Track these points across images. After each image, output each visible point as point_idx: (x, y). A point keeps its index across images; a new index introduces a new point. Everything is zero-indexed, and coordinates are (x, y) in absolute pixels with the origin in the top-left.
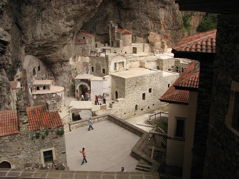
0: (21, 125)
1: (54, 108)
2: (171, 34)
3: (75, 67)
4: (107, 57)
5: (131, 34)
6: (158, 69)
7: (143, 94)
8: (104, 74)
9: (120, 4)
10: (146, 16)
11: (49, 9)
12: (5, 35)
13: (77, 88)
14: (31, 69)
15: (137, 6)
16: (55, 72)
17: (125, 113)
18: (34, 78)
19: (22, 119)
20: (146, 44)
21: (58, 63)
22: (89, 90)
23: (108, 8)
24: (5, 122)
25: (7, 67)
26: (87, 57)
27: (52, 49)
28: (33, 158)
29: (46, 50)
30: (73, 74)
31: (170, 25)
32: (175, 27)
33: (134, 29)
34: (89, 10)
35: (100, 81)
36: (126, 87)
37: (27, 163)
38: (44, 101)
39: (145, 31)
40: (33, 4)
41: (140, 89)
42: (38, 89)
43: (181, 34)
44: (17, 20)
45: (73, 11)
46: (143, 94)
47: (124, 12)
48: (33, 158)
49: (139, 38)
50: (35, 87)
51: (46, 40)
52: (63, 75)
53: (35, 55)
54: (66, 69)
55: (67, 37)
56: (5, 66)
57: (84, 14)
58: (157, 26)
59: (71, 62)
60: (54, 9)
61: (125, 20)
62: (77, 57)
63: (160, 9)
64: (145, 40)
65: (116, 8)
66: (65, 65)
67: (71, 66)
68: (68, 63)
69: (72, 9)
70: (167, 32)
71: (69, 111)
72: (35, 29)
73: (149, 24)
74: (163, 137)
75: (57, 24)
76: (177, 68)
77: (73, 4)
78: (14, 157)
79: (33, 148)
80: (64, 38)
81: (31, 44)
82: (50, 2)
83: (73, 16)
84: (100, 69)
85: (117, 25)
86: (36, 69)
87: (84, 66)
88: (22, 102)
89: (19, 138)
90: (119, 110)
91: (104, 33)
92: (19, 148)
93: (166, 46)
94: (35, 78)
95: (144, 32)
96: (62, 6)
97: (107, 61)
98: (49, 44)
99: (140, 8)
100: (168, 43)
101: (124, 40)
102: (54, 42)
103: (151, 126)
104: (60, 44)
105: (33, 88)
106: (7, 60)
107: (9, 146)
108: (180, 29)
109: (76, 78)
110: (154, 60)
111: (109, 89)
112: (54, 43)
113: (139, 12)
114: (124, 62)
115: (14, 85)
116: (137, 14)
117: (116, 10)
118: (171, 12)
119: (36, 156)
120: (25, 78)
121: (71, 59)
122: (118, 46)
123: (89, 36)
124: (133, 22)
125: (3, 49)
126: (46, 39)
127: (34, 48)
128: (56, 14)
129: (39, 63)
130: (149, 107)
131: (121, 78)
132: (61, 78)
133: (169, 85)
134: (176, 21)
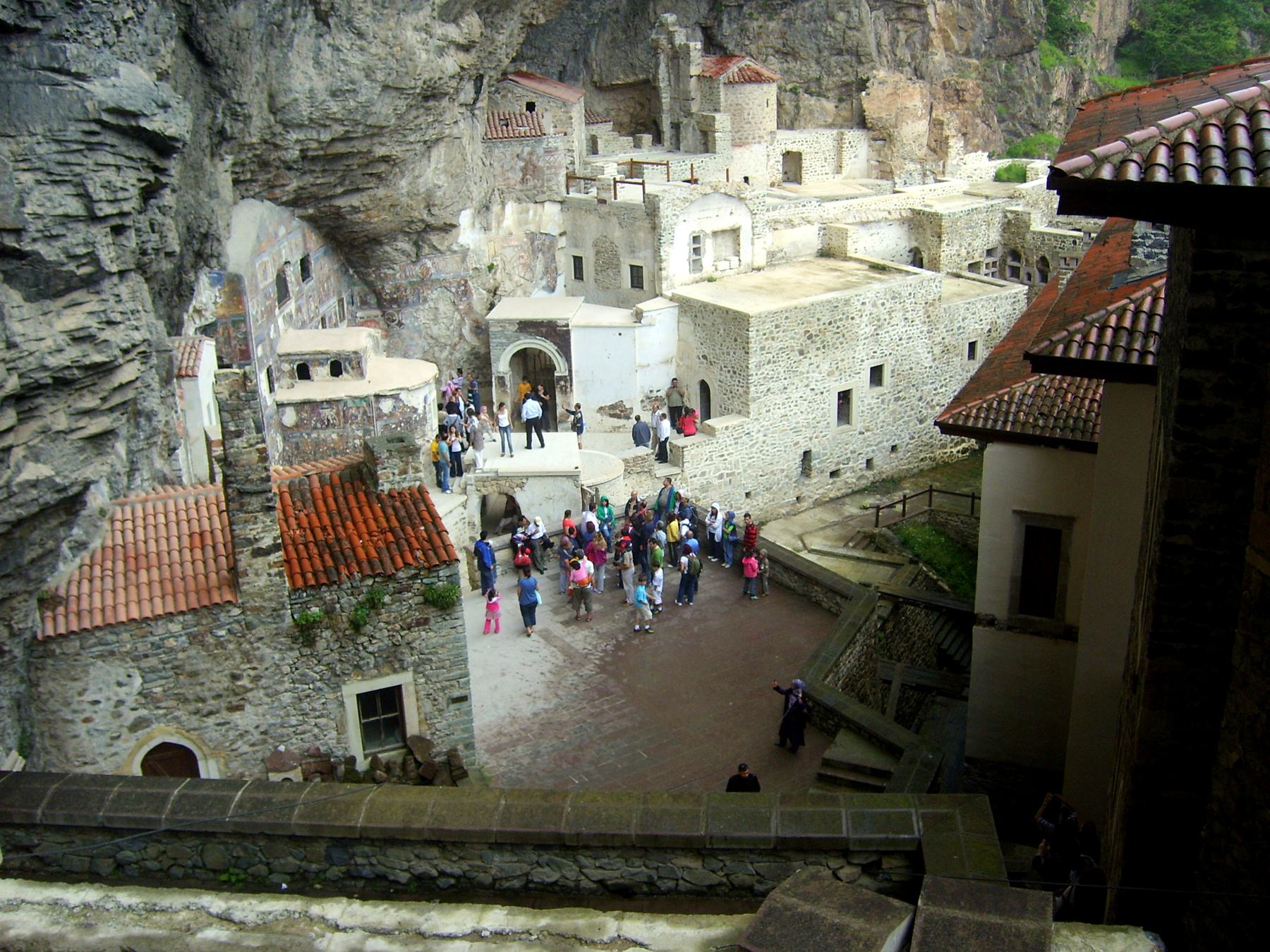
0: (244, 559)
1: (404, 472)
2: (984, 79)
3: (486, 261)
4: (651, 208)
5: (769, 80)
6: (914, 263)
8: (636, 292)
12: (165, 106)
13: (502, 365)
14: (265, 271)
16: (388, 288)
17: (748, 495)
18: (280, 320)
19: (251, 531)
20: (855, 137)
21: (400, 237)
22: (561, 378)
24: (164, 547)
25: (154, 267)
26: (547, 204)
27: (367, 165)
28: (306, 727)
29: (340, 174)
30: (479, 297)
31: (978, 30)
32: (1005, 39)
33: (786, 53)
35: (620, 331)
36: (753, 361)
37: (276, 753)
38: (334, 436)
41: (825, 367)
42: (303, 372)
43: (1033, 79)
44: (191, 19)
48: (306, 727)
49: (813, 101)
50: (286, 367)
51: (340, 121)
52: (425, 300)
53: (285, 199)
54: (442, 267)
55: (445, 102)
56: (146, 259)
58: (908, 38)
59: (468, 234)
62: (496, 208)
66: (435, 248)
67: (465, 253)
68: (449, 238)
71: (466, 485)
72: (284, 66)
73: (869, 28)
76: (1016, 255)
78: (211, 721)
81: (266, 142)
84: (618, 266)
85: (699, 34)
86: (293, 274)
88: (251, 446)
89: (236, 626)
90: (721, 477)
91: (631, 79)
92: (235, 677)
93: (956, 144)
95: (842, 69)
97: (654, 227)
98: (355, 143)
101: (737, 113)
103: (885, 558)
104: (412, 138)
105: (279, 370)
106: (156, 228)
108: (1030, 49)
109: (493, 315)
110: (896, 215)
111: (664, 368)
112: (383, 135)
115: (186, 356)
119: (321, 716)
120: (239, 320)
121: (465, 218)
122: (705, 144)
124: (784, 16)
125: (151, 177)
126: (339, 116)
130: (869, 462)
131: (727, 311)
132: (417, 318)
133: (972, 346)
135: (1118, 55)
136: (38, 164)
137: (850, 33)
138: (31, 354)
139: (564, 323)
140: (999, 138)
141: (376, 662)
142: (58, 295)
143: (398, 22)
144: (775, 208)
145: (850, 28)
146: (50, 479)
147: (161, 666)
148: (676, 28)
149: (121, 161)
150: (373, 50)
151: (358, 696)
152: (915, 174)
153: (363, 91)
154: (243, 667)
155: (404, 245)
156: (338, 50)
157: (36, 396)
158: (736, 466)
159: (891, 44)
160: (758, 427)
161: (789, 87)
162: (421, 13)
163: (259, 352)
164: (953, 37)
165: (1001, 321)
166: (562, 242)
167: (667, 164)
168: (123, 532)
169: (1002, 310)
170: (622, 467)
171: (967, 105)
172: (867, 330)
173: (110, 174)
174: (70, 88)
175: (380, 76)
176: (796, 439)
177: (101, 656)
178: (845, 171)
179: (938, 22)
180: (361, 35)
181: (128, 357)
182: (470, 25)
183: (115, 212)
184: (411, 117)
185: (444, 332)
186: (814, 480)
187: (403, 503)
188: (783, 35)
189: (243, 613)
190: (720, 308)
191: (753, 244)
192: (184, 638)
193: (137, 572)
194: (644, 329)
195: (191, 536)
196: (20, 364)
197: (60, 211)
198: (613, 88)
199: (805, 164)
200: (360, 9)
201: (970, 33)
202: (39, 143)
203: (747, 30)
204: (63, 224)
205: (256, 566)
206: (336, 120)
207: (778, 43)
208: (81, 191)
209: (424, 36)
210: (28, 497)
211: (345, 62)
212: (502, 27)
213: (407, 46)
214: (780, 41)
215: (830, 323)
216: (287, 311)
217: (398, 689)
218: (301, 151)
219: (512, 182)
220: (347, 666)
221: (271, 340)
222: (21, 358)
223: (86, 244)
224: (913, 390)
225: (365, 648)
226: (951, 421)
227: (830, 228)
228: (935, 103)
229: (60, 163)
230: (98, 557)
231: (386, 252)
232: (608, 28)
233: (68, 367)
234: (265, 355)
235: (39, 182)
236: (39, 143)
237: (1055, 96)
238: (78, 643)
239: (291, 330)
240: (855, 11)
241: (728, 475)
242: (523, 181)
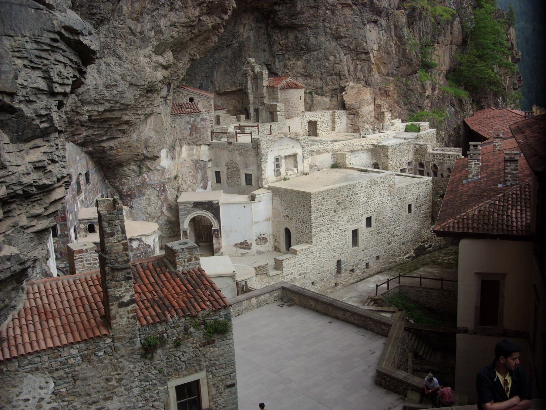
0: (114, 309)
1: (190, 260)
3: (174, 175)
4: (256, 145)
5: (301, 87)
7: (353, 231)
8: (249, 187)
9: (272, 16)
10: (334, 43)
11: (116, 21)
13: (185, 225)
15: (314, 19)
16: (125, 189)
17: (313, 283)
18: (79, 202)
21: (132, 163)
22: (215, 230)
23: (242, 27)
27: (118, 125)
31: (392, 64)
32: (404, 68)
33: (307, 75)
34: (209, 24)
36: (313, 216)
39: (334, 81)
40: (78, 7)
41: (346, 218)
43: (417, 86)
45: (173, 28)
46: (353, 231)
47: (281, 35)
49: (319, 98)
50: (82, 226)
52: (144, 195)
53: (79, 141)
54: (153, 178)
55: (155, 95)
57: (197, 36)
58: (362, 68)
59: (165, 161)
60: (128, 21)
61: (284, 55)
62: (178, 148)
63: (368, 26)
64: (335, 103)
65: (260, 28)
66: (148, 168)
67: (163, 170)
68: (156, 163)
69: (169, 23)
70: (388, 82)
73: (344, 63)
74: (414, 338)
75: (135, 60)
76: (421, 165)
77: (171, 10)
79: (146, 377)
80: (148, 97)
82: (118, 3)
83: (172, 40)
84: (239, 175)
85: (265, 67)
86: (82, 179)
87: (196, 169)
88: (119, 241)
89: (109, 349)
90: (300, 275)
91: (234, 89)
92: (108, 380)
93: (388, 115)
94: (82, 202)
95: (332, 82)
96: (148, 14)
98: (115, 113)
99: (321, 24)
100: (390, 106)
101: (287, 102)
102: (128, 105)
104: (140, 112)
105: (79, 228)
107: (81, 376)
108: (416, 72)
110: (366, 147)
111: (266, 222)
113: (318, 34)
114: (297, 154)
116: (313, 40)
117: (262, 31)
118: (393, 34)
121: (163, 153)
123: (204, 96)
124: (304, 58)
126: (108, 98)
127: (77, 123)
128: (134, 34)
129: (87, 164)
130: (367, 265)
131: (299, 192)
133: (410, 206)
134: (404, 55)
135: (447, 79)
136: (25, 55)
137: (336, 65)
138: (13, 174)
139: (216, 202)
140: (405, 112)
141: (186, 367)
142: (27, 141)
143: (137, 53)
144: (311, 145)
145: (336, 63)
146: (17, 254)
147: (65, 375)
148: (255, 64)
149: (67, 62)
150: (126, 66)
151: (176, 387)
152: (370, 130)
153: (121, 86)
154: (112, 373)
155: (134, 167)
156: (109, 65)
157: (11, 203)
158: (307, 269)
159: (354, 70)
160: (316, 249)
161: (308, 91)
162: (147, 49)
163: (70, 217)
164: (381, 68)
165: (421, 194)
166: (210, 164)
167: (258, 126)
168: (35, 299)
169: (422, 189)
170: (254, 271)
171: (391, 98)
172: (364, 199)
173: (60, 67)
174: (45, 12)
175: (129, 79)
176: (334, 254)
177: (31, 371)
178: (337, 130)
179: (375, 60)
180: (120, 58)
181: (59, 184)
182: (168, 56)
183: (62, 91)
184: (140, 101)
185: (154, 210)
186: (343, 275)
187: (192, 277)
188: (304, 67)
189: (113, 341)
190: (295, 191)
191: (303, 162)
192: (79, 358)
193: (47, 321)
194: (257, 203)
195: (75, 300)
196: (7, 179)
197: (35, 85)
198: (225, 94)
199: (319, 126)
200: (120, 45)
201: (389, 66)
202: (27, 42)
203: (288, 65)
204: (36, 94)
205: (121, 313)
206: (107, 101)
207: (302, 71)
208: (46, 75)
209: (149, 60)
210: (5, 267)
211: (112, 71)
212: (181, 60)
213: (141, 64)
214: (303, 70)
215: (347, 197)
216: (81, 198)
217: (197, 383)
218: (89, 116)
219: (185, 135)
220: (170, 370)
221: (75, 212)
222: (8, 175)
223: (47, 108)
224: (385, 229)
225: (180, 358)
226: (441, 230)
227: (337, 154)
228: (376, 97)
229: (37, 57)
230: (23, 313)
231: (125, 171)
232: (222, 66)
233: (31, 185)
234: (73, 219)
235: (25, 66)
236: (27, 42)
237: (427, 94)
238: (17, 364)
239: (83, 208)
240: (338, 55)
241: (303, 274)
242: (191, 135)
